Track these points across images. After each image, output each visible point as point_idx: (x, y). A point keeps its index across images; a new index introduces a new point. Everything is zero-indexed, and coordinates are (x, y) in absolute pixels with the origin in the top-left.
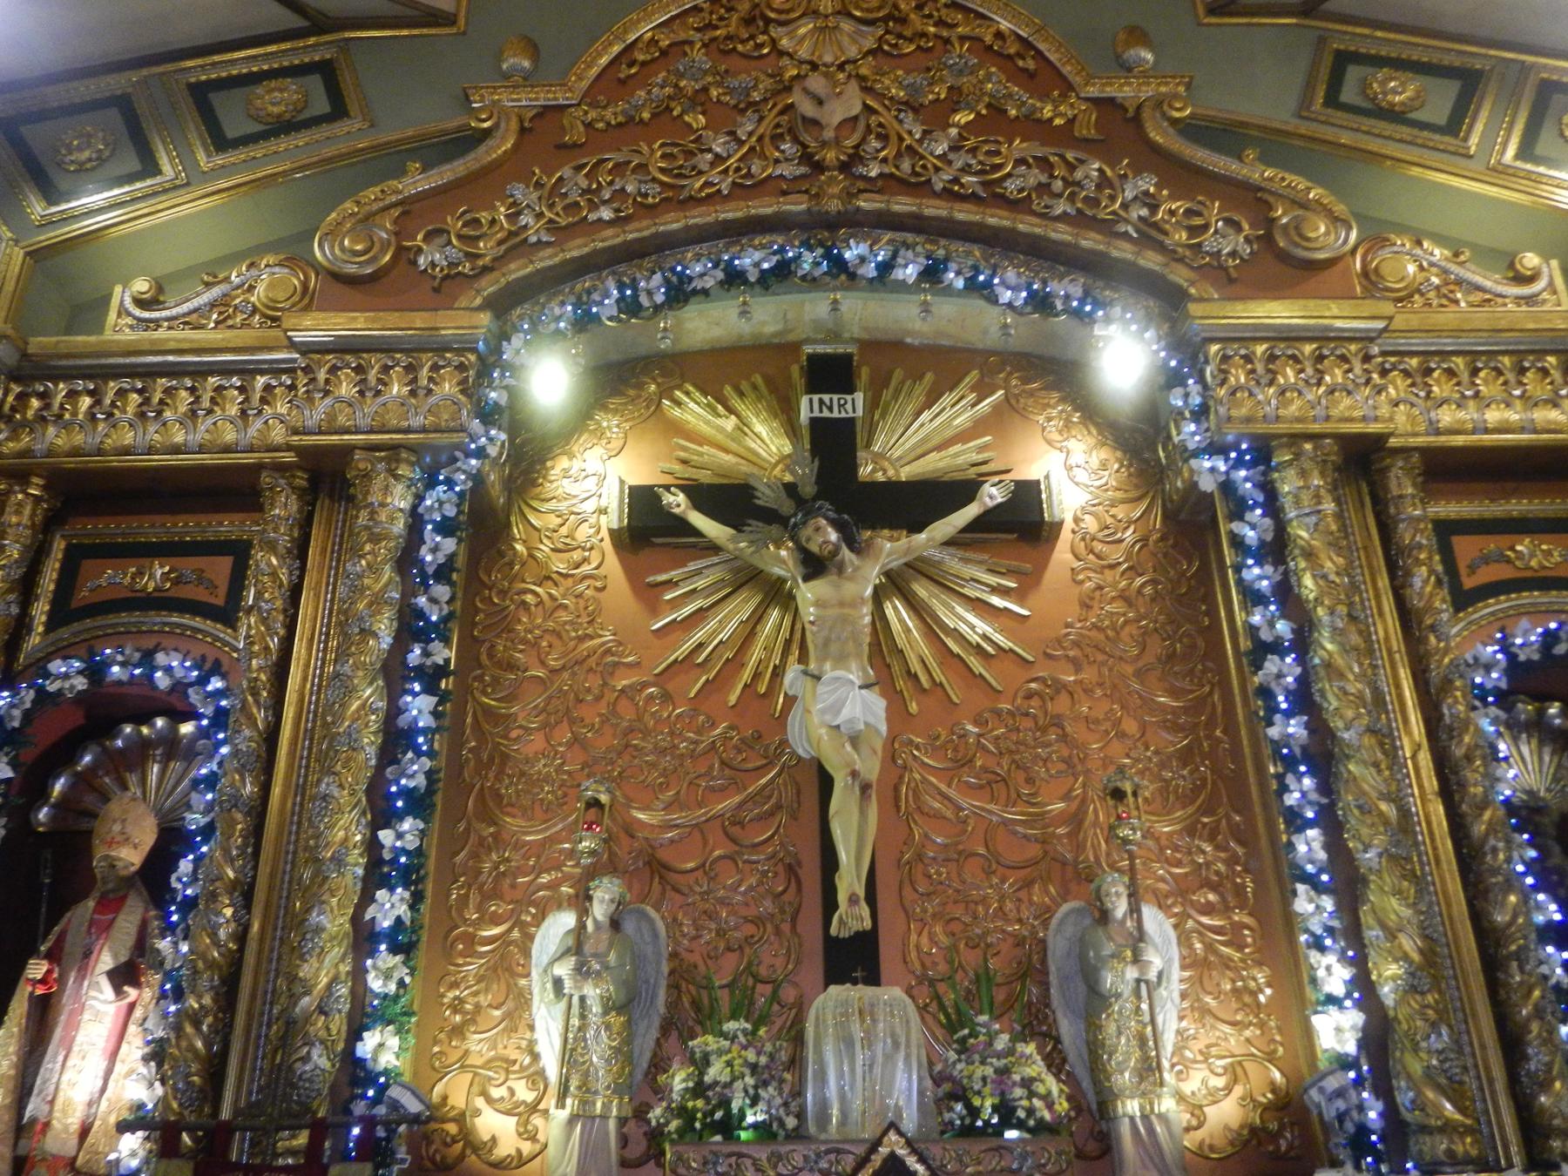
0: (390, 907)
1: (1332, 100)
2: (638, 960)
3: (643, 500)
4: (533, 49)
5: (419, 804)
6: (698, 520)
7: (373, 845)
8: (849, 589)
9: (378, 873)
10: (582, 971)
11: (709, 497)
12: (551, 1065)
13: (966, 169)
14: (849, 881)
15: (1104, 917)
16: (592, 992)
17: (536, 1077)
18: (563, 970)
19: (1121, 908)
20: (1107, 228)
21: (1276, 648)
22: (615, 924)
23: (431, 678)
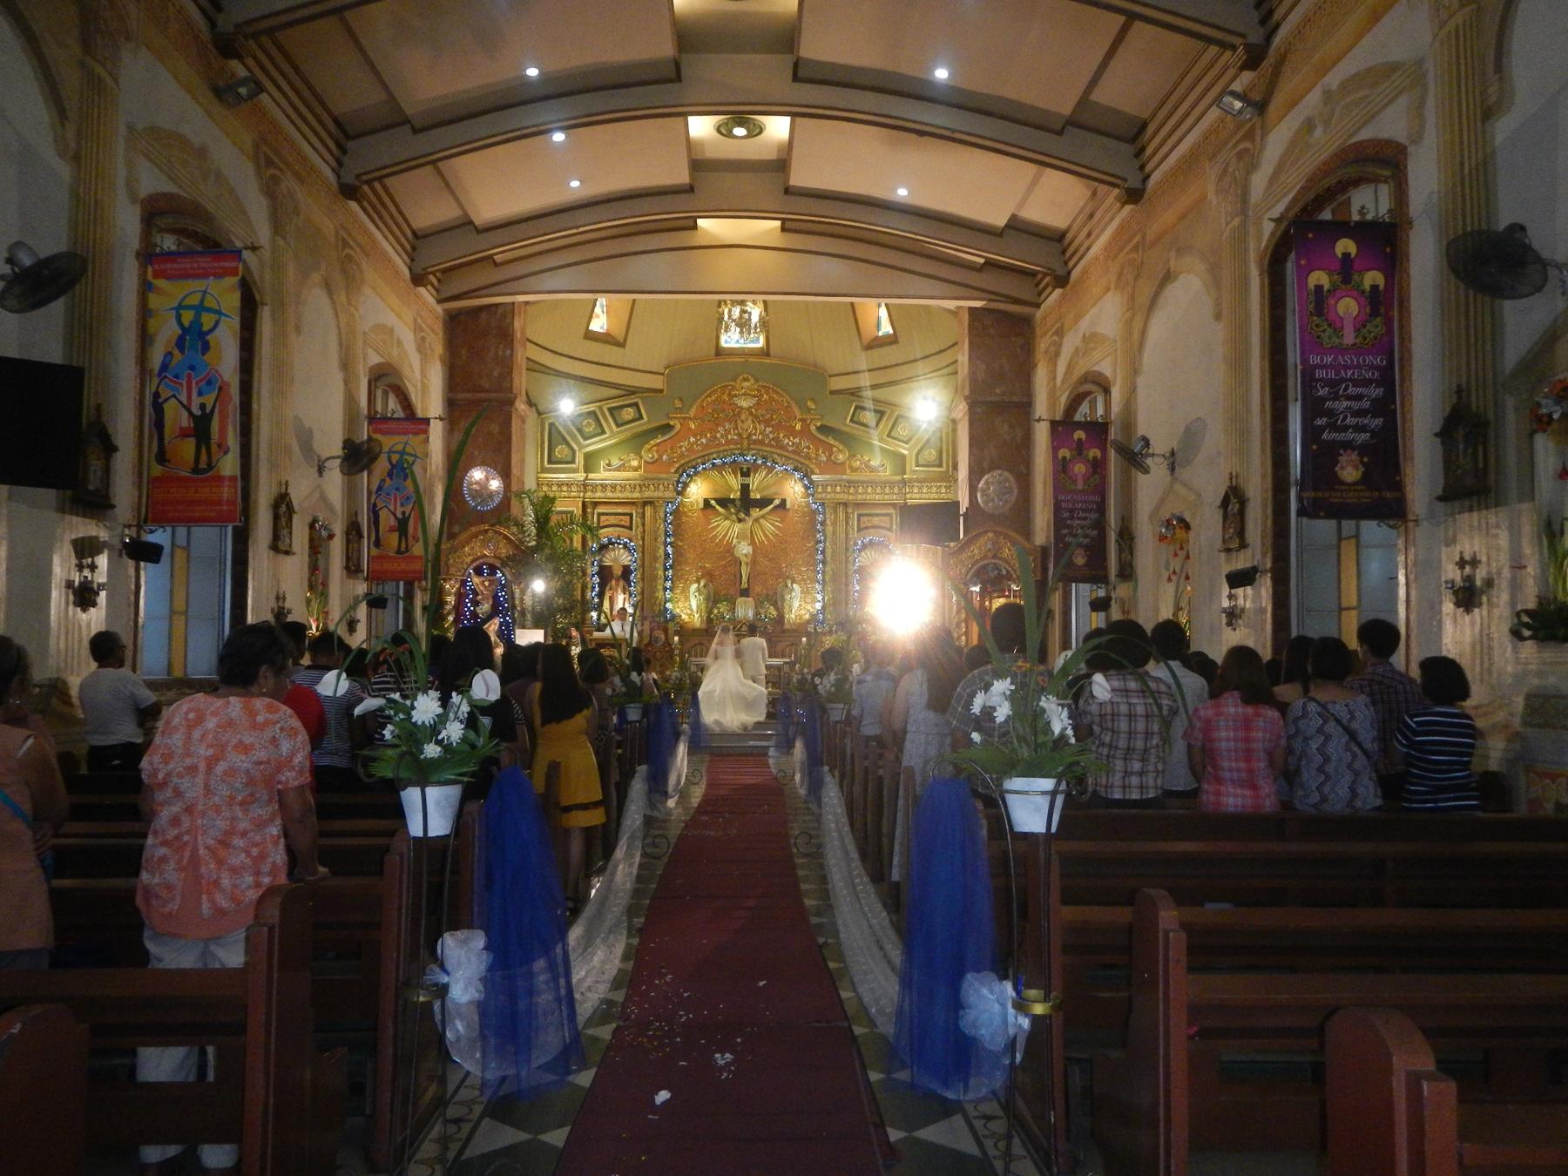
0: (669, 584)
1: (851, 421)
3: (707, 502)
4: (681, 400)
6: (718, 507)
9: (666, 579)
11: (719, 502)
12: (694, 608)
14: (744, 579)
17: (691, 609)
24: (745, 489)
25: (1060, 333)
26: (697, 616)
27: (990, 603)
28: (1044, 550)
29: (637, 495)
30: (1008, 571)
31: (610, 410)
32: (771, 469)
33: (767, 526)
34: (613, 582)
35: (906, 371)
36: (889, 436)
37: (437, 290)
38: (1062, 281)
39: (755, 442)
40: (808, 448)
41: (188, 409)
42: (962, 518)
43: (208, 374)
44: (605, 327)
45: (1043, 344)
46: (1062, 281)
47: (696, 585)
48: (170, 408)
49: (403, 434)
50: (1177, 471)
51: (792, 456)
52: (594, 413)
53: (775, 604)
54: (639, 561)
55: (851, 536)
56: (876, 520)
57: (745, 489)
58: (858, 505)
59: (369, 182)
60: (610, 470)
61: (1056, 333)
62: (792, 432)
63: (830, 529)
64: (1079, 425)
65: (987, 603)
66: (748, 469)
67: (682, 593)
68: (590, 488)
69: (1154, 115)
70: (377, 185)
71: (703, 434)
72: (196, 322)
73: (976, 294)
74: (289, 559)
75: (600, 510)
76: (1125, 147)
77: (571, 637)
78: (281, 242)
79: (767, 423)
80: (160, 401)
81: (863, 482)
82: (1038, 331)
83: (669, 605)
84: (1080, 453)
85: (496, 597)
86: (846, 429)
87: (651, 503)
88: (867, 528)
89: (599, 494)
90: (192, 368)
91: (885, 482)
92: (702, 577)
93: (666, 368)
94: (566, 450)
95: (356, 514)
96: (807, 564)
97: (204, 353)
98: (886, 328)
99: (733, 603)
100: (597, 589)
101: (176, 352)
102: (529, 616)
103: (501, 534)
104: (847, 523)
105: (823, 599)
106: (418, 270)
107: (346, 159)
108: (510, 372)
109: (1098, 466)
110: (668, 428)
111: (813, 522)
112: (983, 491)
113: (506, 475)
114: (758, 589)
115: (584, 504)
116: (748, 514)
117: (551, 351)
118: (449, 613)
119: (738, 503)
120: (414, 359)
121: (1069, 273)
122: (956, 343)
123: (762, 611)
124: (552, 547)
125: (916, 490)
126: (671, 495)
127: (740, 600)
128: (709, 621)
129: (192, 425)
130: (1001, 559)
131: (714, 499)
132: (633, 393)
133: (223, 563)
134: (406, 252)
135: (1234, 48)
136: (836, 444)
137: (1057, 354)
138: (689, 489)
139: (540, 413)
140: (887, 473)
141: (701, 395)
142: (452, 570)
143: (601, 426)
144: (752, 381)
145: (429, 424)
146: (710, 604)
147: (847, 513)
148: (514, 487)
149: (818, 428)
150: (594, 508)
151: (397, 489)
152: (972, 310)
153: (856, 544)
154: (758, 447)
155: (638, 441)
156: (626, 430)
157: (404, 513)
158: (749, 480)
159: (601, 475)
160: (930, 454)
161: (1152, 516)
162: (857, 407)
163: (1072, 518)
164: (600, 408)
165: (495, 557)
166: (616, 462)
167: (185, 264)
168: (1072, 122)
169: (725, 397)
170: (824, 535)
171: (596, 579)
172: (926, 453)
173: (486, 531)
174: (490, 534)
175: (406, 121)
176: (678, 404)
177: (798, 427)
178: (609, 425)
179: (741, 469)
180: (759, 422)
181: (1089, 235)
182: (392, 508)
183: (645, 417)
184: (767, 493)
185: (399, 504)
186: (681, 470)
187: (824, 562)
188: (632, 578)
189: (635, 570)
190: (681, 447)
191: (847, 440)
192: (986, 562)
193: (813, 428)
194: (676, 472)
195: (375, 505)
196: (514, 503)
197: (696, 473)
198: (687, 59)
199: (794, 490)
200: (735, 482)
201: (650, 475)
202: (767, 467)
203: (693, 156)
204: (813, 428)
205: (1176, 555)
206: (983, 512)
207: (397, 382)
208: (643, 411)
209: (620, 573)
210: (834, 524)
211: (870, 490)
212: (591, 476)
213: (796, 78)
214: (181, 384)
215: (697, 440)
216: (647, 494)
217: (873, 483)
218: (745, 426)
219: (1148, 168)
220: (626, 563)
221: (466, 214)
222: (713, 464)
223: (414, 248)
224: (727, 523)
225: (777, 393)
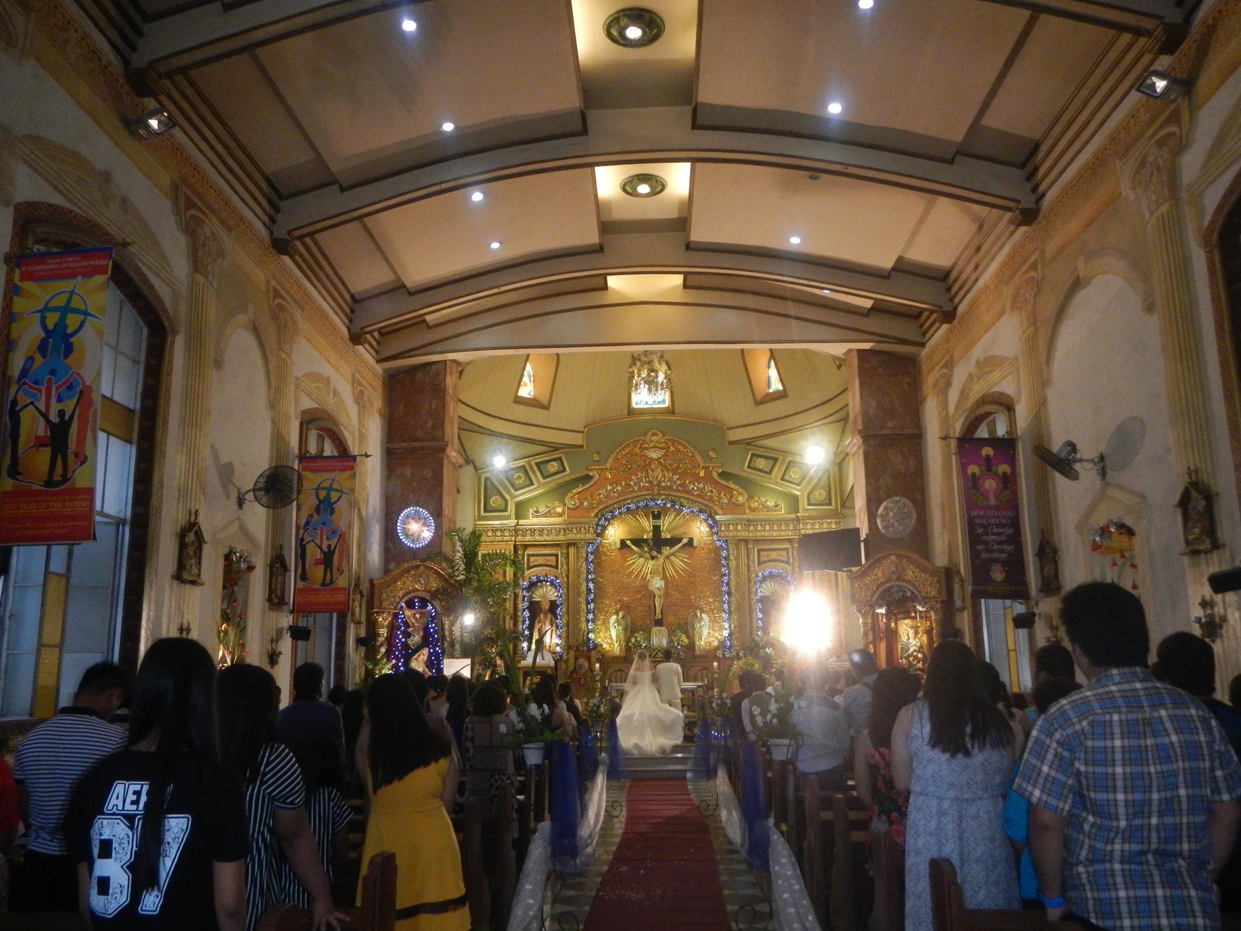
0: (591, 616)
1: (749, 467)
2: (627, 623)
3: (623, 542)
4: (598, 453)
5: (593, 601)
6: (633, 547)
7: (587, 608)
8: (658, 563)
9: (588, 612)
10: (618, 625)
12: (614, 637)
13: (680, 485)
15: (697, 616)
16: (620, 628)
17: (612, 639)
18: (616, 625)
19: (699, 615)
20: (703, 497)
21: (725, 575)
22: (623, 618)
23: (592, 580)
24: (657, 529)
25: (950, 365)
26: (616, 645)
27: (896, 624)
28: (949, 574)
29: (562, 537)
30: (912, 593)
31: (538, 464)
32: (679, 512)
33: (678, 562)
34: (542, 616)
35: (795, 421)
36: (782, 479)
37: (377, 352)
38: (949, 316)
39: (665, 488)
40: (712, 492)
41: (45, 416)
42: (862, 544)
43: (69, 378)
44: (532, 394)
45: (930, 380)
46: (949, 316)
47: (615, 617)
48: (27, 416)
49: (331, 471)
50: (1110, 474)
51: (697, 499)
52: (523, 467)
53: (686, 633)
54: (564, 597)
55: (752, 569)
56: (774, 555)
57: (657, 529)
58: (757, 541)
59: (300, 238)
60: (538, 517)
61: (945, 366)
62: (697, 478)
63: (733, 563)
64: (984, 442)
65: (893, 625)
66: (659, 513)
67: (602, 624)
68: (521, 532)
69: (1045, 137)
70: (308, 240)
71: (619, 483)
72: (61, 324)
73: (865, 336)
74: (196, 591)
75: (530, 551)
76: (1018, 174)
77: (496, 666)
78: (200, 278)
79: (675, 472)
80: (17, 409)
81: (761, 521)
82: (925, 369)
83: (591, 636)
84: (989, 469)
85: (426, 629)
86: (745, 475)
87: (574, 544)
88: (765, 562)
89: (528, 538)
90: (53, 372)
91: (781, 520)
92: (621, 609)
93: (585, 427)
94: (500, 500)
95: (281, 547)
96: (714, 595)
97: (66, 357)
98: (776, 385)
99: (648, 631)
100: (527, 622)
101: (38, 357)
102: (458, 647)
103: (432, 569)
104: (748, 557)
105: (730, 627)
106: (356, 329)
107: (279, 217)
108: (442, 425)
109: (1009, 482)
110: (587, 478)
111: (717, 559)
112: (882, 517)
113: (438, 514)
114: (670, 619)
115: (515, 547)
116: (660, 552)
117: (485, 414)
118: (381, 645)
119: (651, 543)
120: (353, 411)
121: (955, 309)
122: (846, 389)
123: (675, 639)
124: (479, 581)
126: (591, 537)
127: (655, 629)
128: (628, 649)
129: (49, 433)
130: (904, 580)
131: (630, 540)
132: (557, 449)
133: (114, 593)
134: (346, 314)
135: (1149, 33)
136: (736, 487)
137: (948, 384)
138: (607, 532)
139: (476, 469)
140: (783, 512)
141: (616, 449)
142: (385, 604)
144: (660, 435)
145: (355, 460)
146: (628, 634)
147: (748, 548)
148: (445, 528)
149: (719, 474)
150: (524, 550)
151: (324, 524)
152: (861, 352)
153: (757, 576)
154: (667, 493)
155: (562, 490)
156: (551, 482)
157: (329, 546)
158: (660, 522)
159: (531, 521)
160: (820, 495)
161: (1080, 527)
162: (753, 455)
163: (987, 534)
165: (426, 590)
166: (542, 509)
167: (52, 264)
168: (963, 152)
169: (637, 450)
170: (728, 568)
171: (527, 614)
172: (817, 493)
173: (418, 566)
174: (422, 569)
175: (335, 182)
176: (596, 457)
177: (702, 474)
178: (537, 477)
179: (653, 512)
180: (668, 470)
181: (977, 267)
182: (318, 542)
183: (567, 469)
184: (677, 533)
185: (325, 537)
186: (601, 515)
187: (729, 593)
188: (558, 611)
189: (561, 604)
190: (599, 494)
191: (745, 483)
192: (890, 584)
193: (715, 475)
194: (596, 516)
195: (302, 539)
196: (445, 540)
197: (613, 517)
198: (591, 115)
199: (699, 530)
200: (647, 524)
201: (572, 520)
202: (675, 510)
203: (603, 219)
204: (715, 475)
205: (1115, 564)
206: (883, 535)
207: (334, 428)
208: (566, 466)
209: (547, 607)
210: (737, 558)
211: (767, 527)
212: (521, 522)
213: (695, 126)
214: (40, 390)
215: (614, 488)
216: (570, 536)
217: (770, 522)
218: (655, 474)
219: (1042, 188)
220: (553, 599)
221: (399, 278)
222: (628, 509)
223: (352, 311)
224: (642, 560)
225: (682, 445)
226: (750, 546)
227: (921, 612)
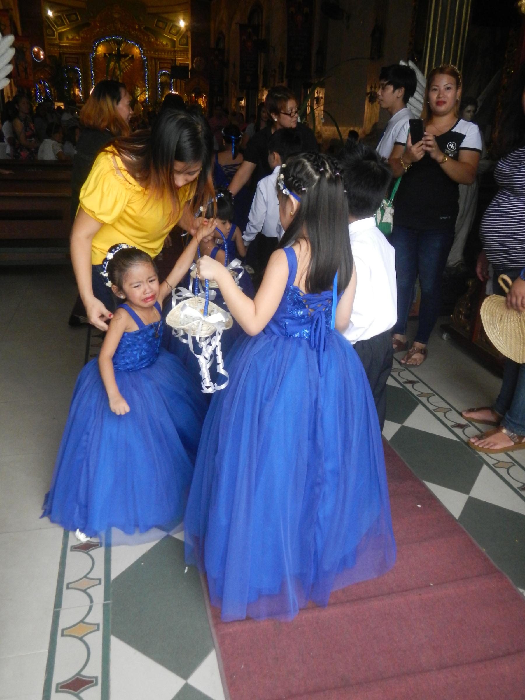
3: (105, 54)
24: (118, 49)
31: (66, 15)
36: (169, 32)
56: (166, 65)
58: (159, 59)
63: (150, 68)
65: (197, 100)
110: (88, 25)
111: (144, 65)
115: (60, 53)
125: (179, 54)
140: (169, 47)
143: (64, 22)
153: (159, 74)
162: (157, 20)
164: (63, 15)
166: (70, 37)
177: (137, 27)
187: (148, 80)
193: (142, 28)
199: (136, 51)
211: (163, 53)
217: (164, 51)
226: (157, 61)
227: (204, 96)
